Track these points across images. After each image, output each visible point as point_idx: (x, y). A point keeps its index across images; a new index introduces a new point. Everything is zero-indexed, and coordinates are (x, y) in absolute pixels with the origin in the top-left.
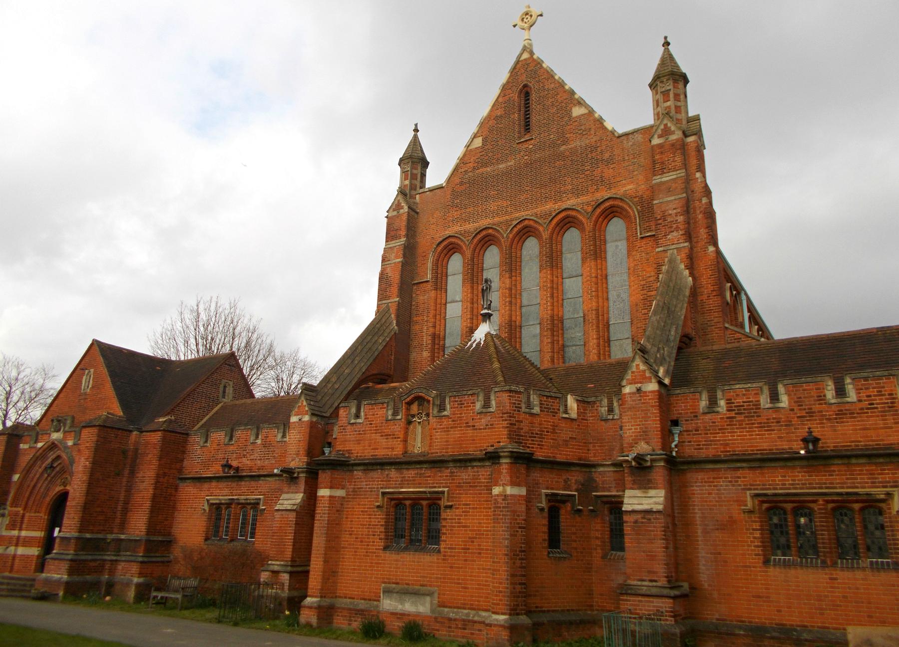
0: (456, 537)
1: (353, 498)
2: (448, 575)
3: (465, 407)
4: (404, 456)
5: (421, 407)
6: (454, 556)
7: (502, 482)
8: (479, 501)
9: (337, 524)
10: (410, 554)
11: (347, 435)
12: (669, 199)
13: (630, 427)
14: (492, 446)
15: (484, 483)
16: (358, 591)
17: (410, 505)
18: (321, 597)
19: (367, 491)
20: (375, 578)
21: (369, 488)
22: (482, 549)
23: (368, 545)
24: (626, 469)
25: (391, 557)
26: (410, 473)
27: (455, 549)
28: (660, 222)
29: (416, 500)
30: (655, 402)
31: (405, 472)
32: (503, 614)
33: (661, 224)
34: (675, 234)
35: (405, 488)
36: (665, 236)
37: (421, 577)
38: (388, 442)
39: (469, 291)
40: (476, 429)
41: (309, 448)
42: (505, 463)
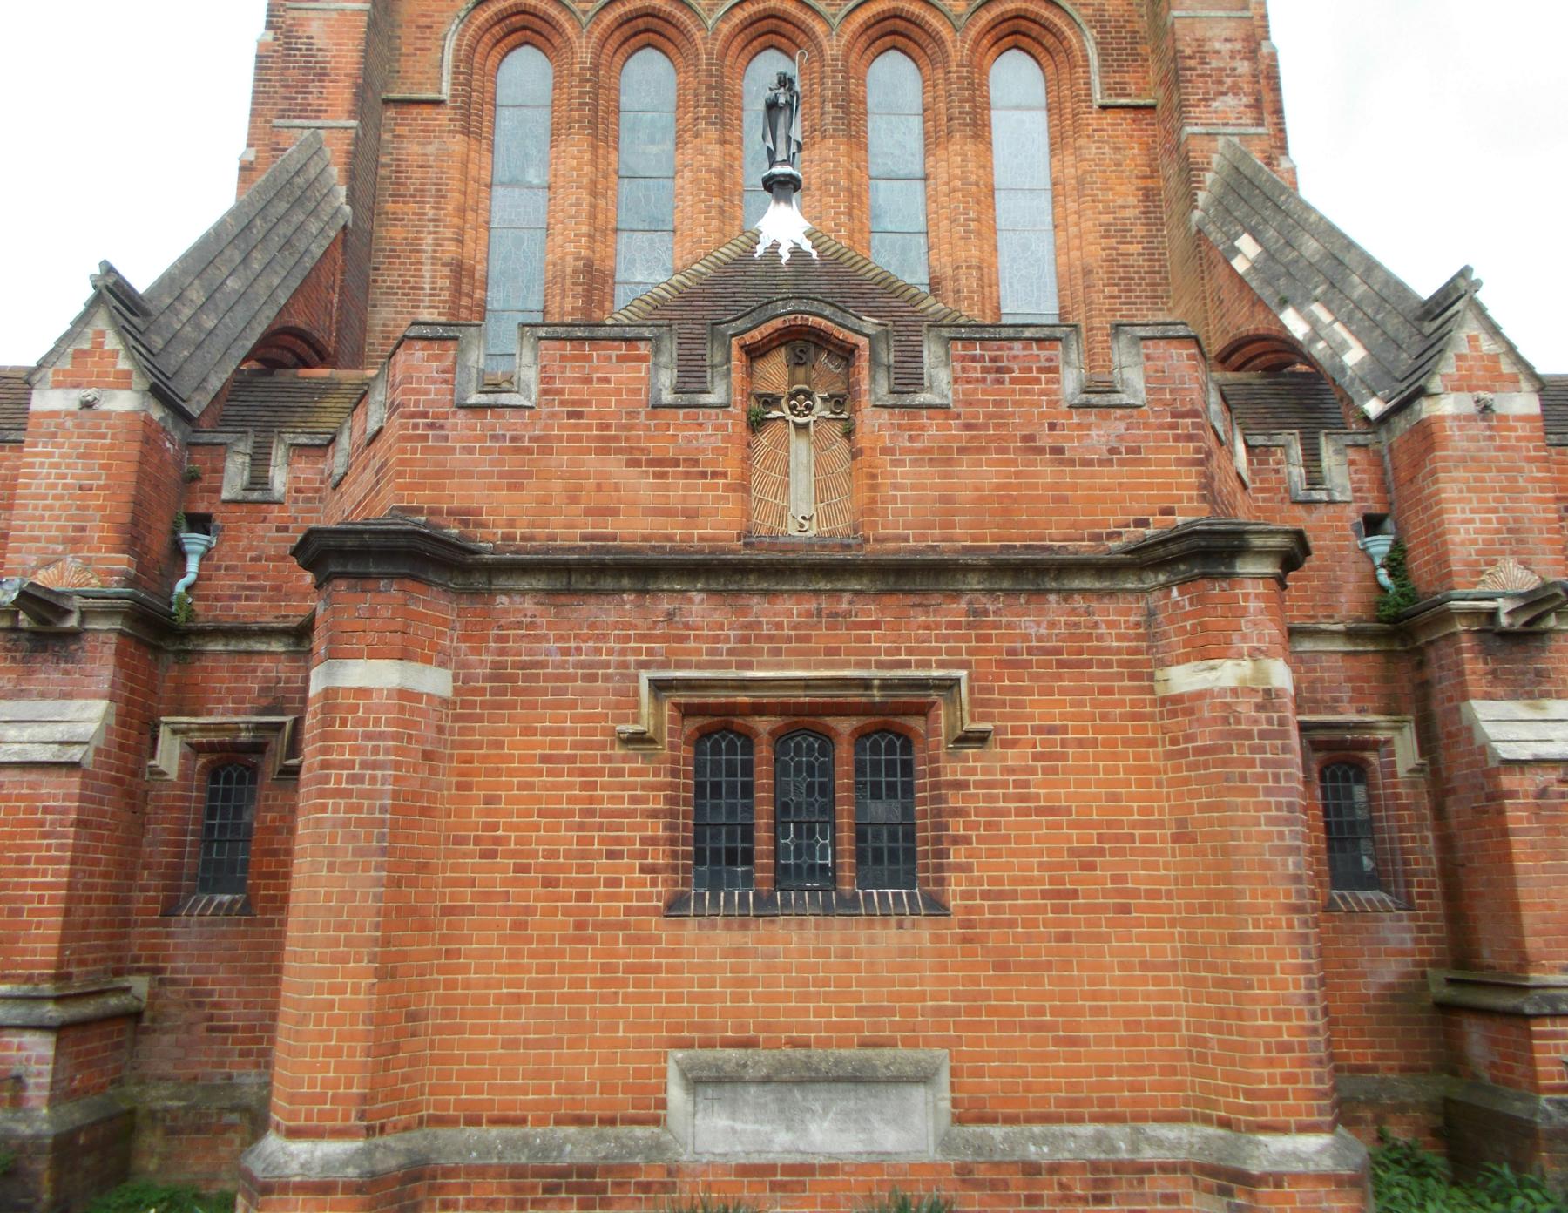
0: (1012, 853)
1: (501, 706)
2: (986, 996)
3: (1013, 381)
4: (746, 545)
5: (801, 372)
6: (1012, 924)
7: (1245, 646)
8: (1104, 717)
9: (424, 812)
10: (801, 925)
11: (452, 450)
12: (1213, 14)
13: (1468, 515)
14: (1143, 523)
15: (1119, 651)
16: (539, 1090)
17: (772, 733)
18: (370, 1131)
19: (574, 678)
20: (630, 1028)
21: (578, 665)
22: (1135, 894)
23: (585, 897)
24: (1464, 637)
27: (1013, 895)
28: (1191, 63)
30: (1536, 449)
31: (757, 604)
32: (1304, 1129)
33: (1194, 69)
34: (1230, 100)
35: (762, 666)
36: (1206, 100)
37: (861, 1011)
38: (667, 488)
39: (587, 156)
40: (1072, 462)
41: (135, 523)
42: (1255, 577)
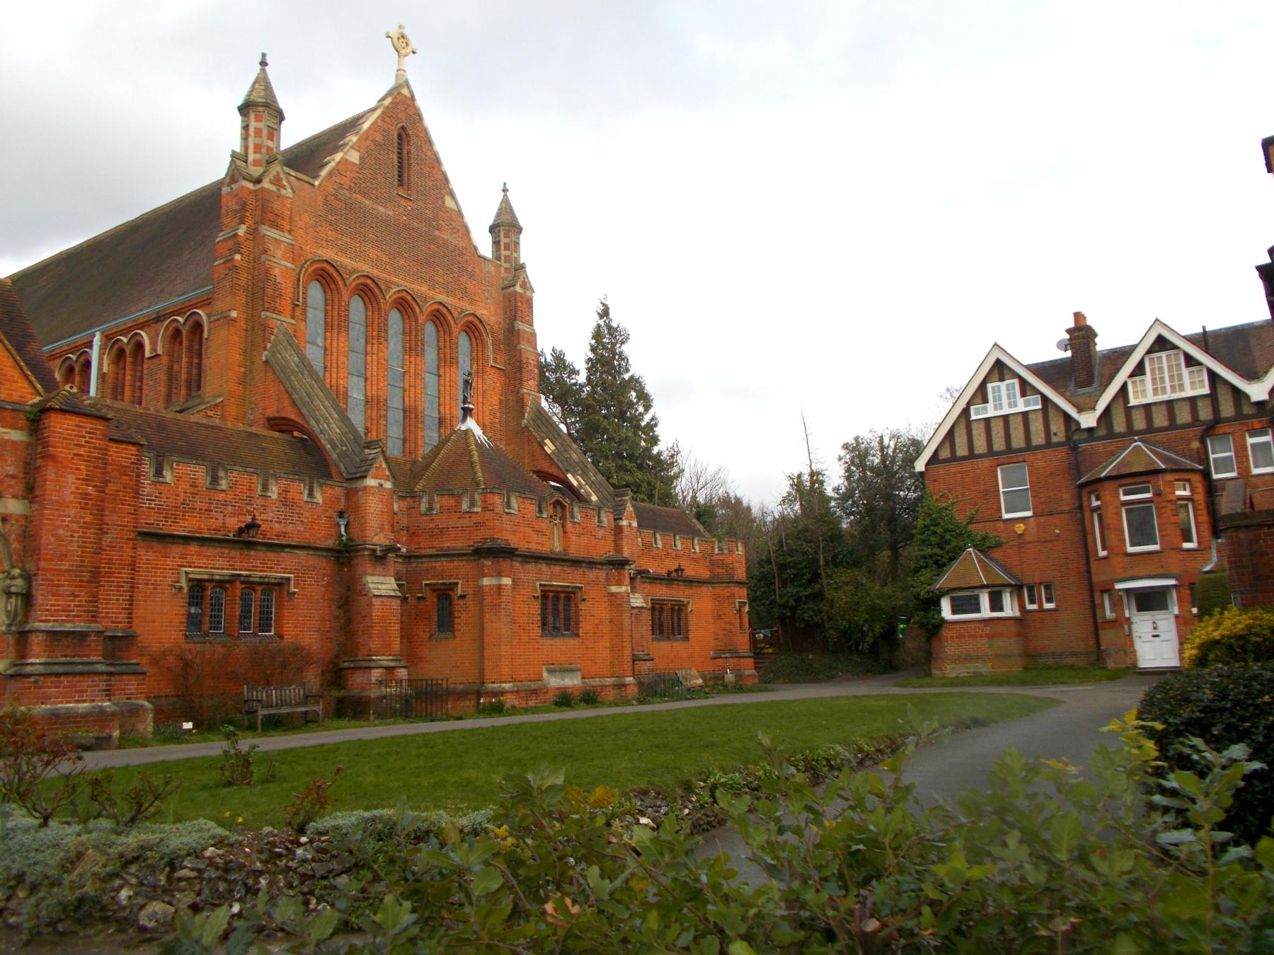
25: (547, 642)
26: (557, 569)
29: (557, 593)
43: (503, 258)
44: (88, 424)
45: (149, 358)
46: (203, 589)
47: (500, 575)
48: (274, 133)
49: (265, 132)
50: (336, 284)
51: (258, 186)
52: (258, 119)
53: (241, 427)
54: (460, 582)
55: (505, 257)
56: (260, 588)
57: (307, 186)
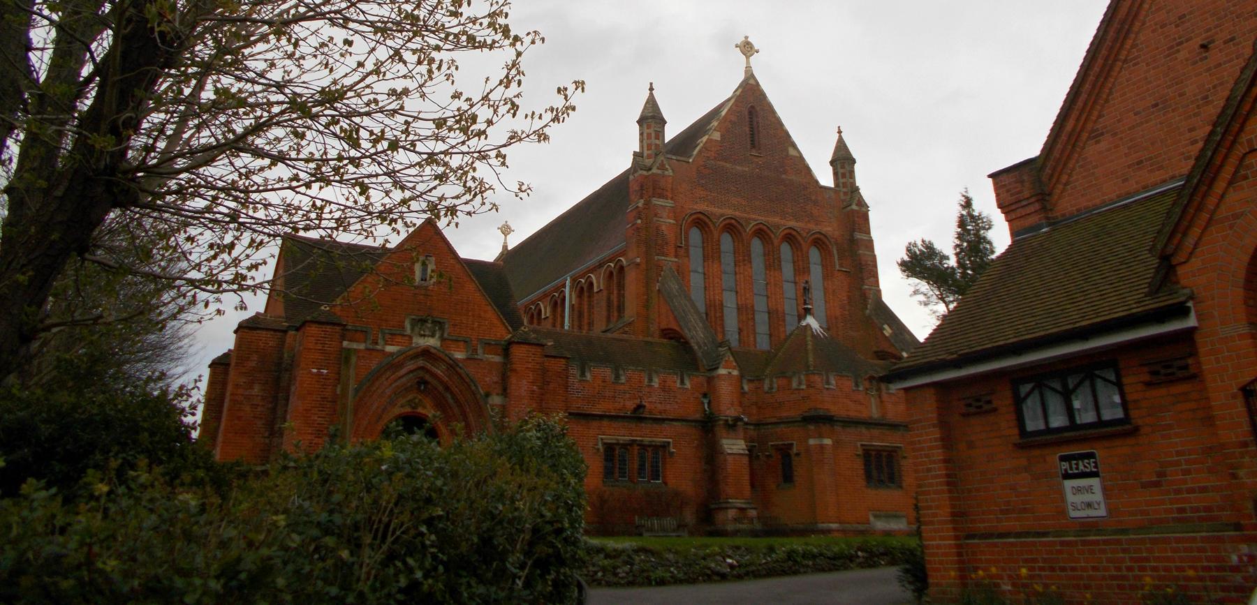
26: (876, 432)
31: (872, 430)
43: (841, 185)
44: (533, 349)
45: (597, 292)
46: (614, 450)
47: (821, 436)
48: (660, 134)
49: (653, 135)
50: (709, 227)
51: (650, 172)
52: (649, 127)
53: (641, 338)
54: (795, 443)
55: (843, 183)
56: (650, 449)
57: (684, 163)
